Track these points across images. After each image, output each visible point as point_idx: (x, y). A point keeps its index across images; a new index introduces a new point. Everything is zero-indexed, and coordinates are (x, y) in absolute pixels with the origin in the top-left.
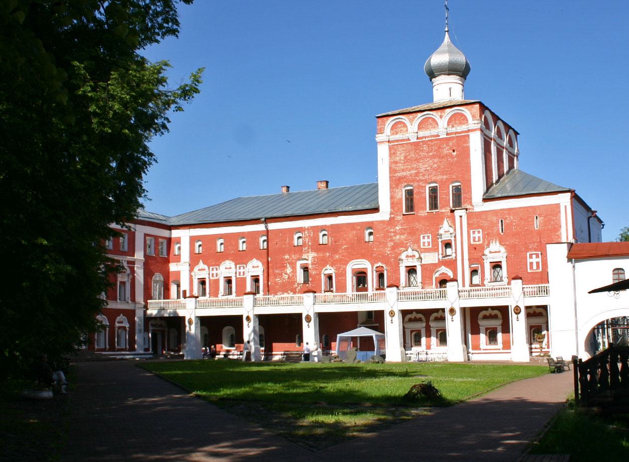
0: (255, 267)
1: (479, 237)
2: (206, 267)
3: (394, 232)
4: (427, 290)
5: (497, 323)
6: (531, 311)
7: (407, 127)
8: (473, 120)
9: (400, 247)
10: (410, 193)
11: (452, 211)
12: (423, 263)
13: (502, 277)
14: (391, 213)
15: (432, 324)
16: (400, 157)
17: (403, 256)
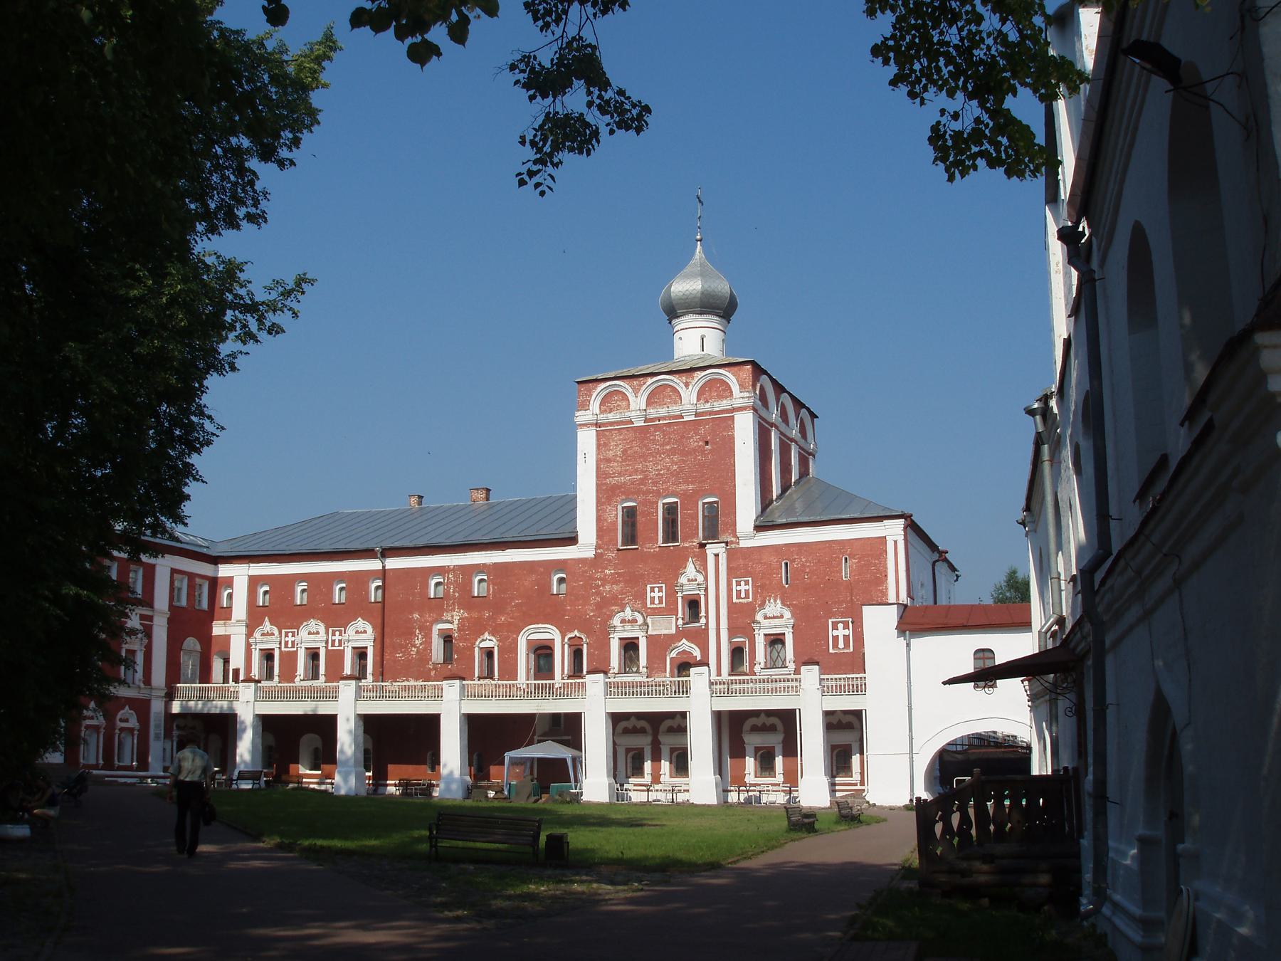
0: (361, 634)
1: (747, 591)
2: (276, 631)
3: (600, 579)
4: (657, 680)
5: (774, 740)
6: (834, 720)
7: (628, 400)
8: (741, 392)
9: (613, 606)
10: (630, 514)
11: (704, 545)
13: (785, 660)
14: (598, 547)
15: (662, 738)
16: (615, 450)
17: (616, 621)
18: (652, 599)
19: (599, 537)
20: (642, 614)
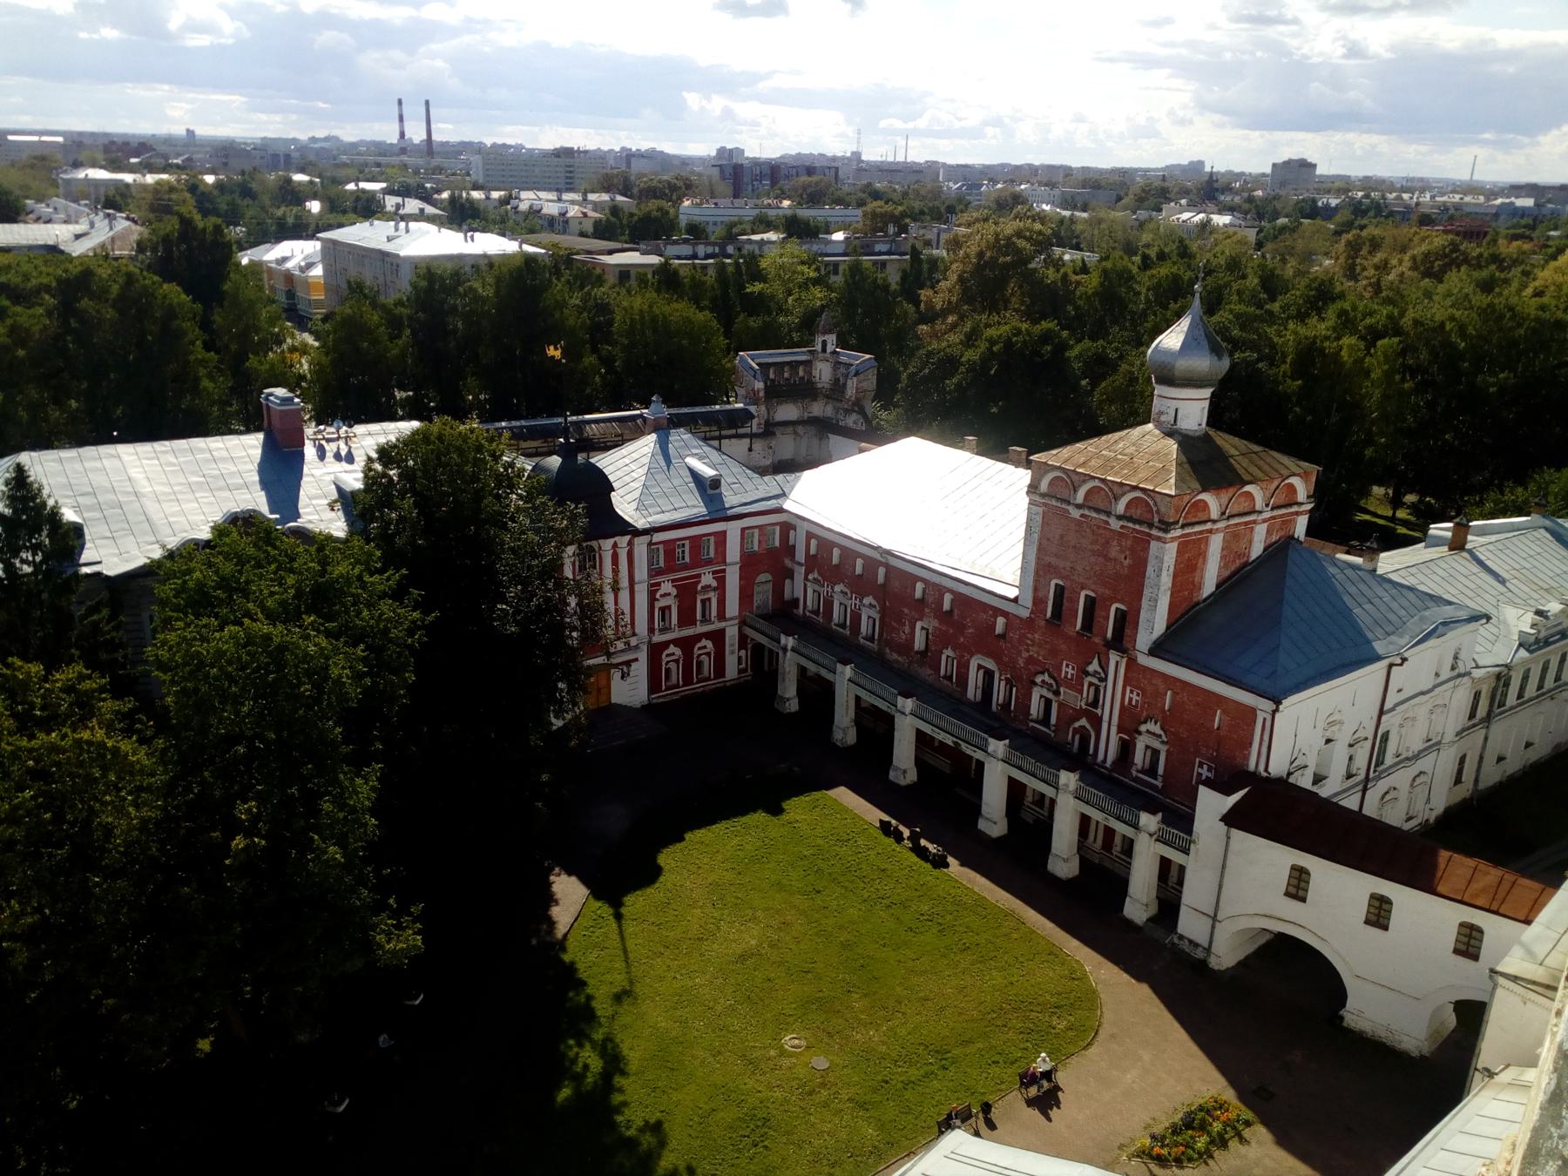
12: (1061, 697)
18: (1067, 673)
19: (1034, 603)
20: (1057, 684)
